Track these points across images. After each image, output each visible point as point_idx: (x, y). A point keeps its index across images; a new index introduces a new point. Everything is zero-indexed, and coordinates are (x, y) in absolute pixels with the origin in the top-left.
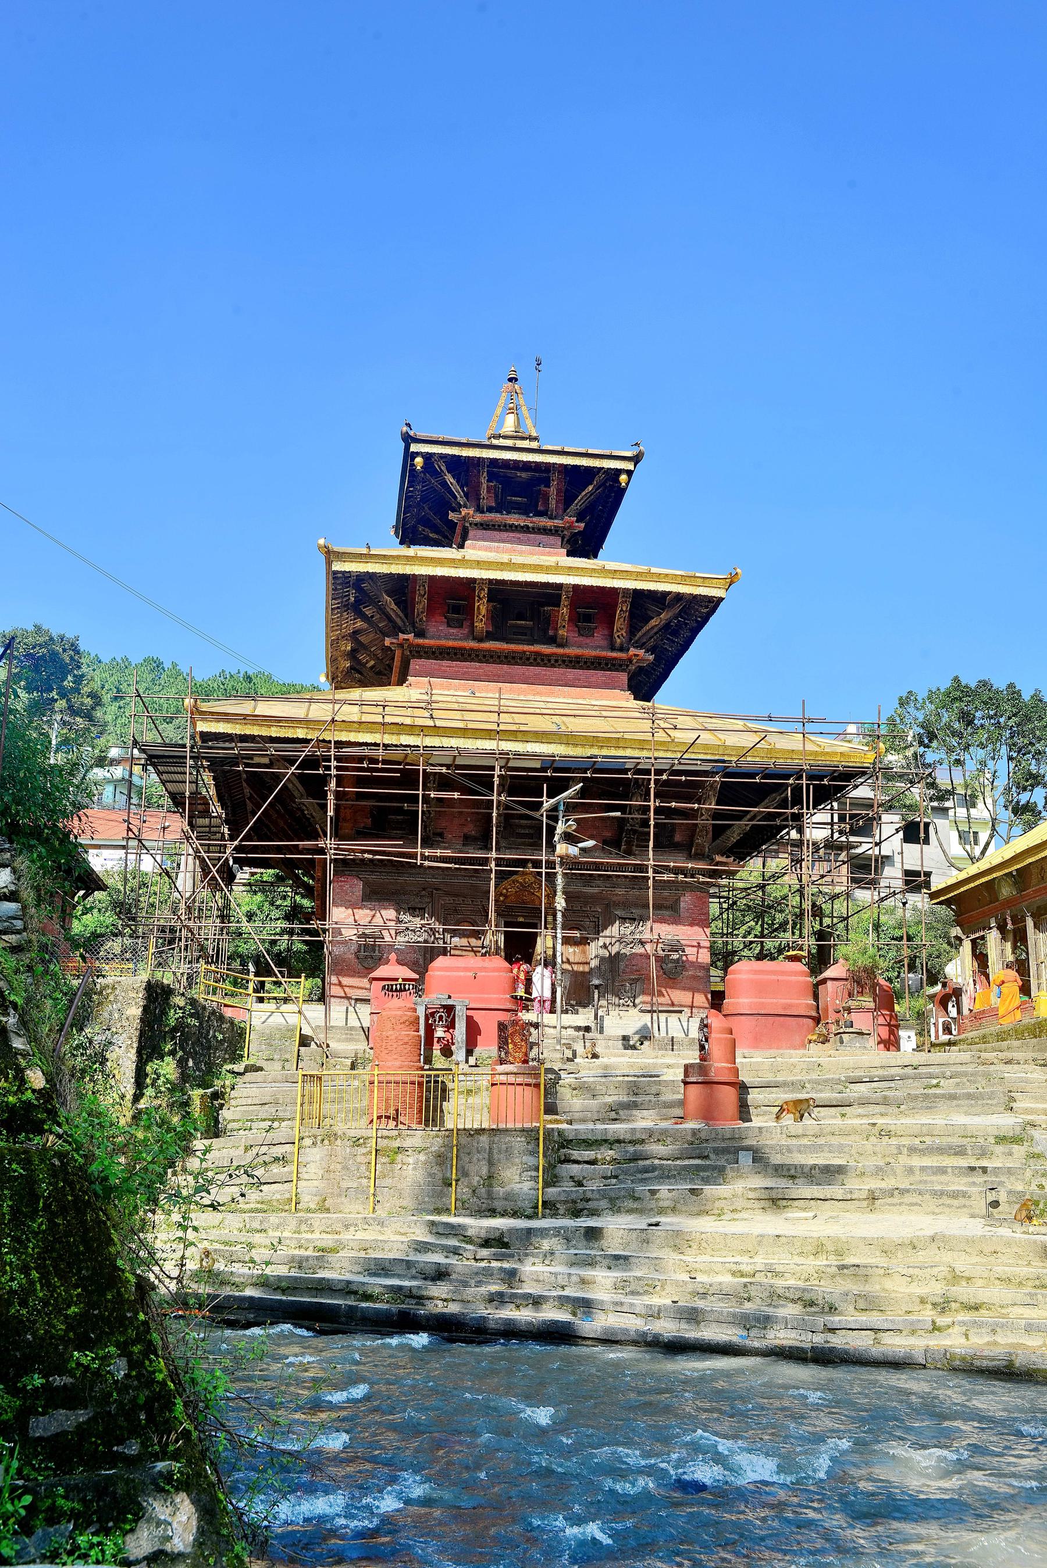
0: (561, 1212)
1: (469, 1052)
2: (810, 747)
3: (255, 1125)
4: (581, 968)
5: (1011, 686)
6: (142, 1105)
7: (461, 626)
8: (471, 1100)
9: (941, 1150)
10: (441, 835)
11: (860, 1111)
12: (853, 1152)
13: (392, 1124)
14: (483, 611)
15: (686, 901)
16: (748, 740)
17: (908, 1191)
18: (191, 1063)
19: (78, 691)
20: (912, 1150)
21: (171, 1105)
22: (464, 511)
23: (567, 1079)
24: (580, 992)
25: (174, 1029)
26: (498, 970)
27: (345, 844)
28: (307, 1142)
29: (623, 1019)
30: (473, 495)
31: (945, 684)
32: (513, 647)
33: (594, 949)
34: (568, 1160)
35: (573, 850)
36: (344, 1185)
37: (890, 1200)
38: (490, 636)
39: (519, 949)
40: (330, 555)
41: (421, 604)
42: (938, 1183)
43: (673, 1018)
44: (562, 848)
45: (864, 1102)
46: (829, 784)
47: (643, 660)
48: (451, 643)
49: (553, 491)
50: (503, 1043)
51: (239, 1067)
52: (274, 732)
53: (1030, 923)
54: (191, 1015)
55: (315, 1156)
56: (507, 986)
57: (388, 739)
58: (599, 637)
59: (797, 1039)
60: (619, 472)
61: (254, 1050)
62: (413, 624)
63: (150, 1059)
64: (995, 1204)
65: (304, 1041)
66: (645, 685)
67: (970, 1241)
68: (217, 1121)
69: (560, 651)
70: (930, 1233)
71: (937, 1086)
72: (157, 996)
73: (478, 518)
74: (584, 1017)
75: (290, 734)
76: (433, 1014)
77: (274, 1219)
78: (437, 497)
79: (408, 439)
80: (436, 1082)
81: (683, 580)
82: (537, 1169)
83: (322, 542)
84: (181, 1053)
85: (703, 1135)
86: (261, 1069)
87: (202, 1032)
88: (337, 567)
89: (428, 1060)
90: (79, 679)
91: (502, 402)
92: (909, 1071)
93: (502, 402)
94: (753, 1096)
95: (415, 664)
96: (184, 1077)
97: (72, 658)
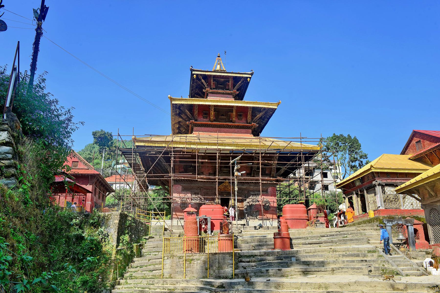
0: (240, 277)
1: (212, 232)
2: (302, 146)
3: (151, 254)
4: (242, 209)
5: (349, 135)
6: (119, 248)
7: (207, 118)
8: (213, 245)
10: (202, 173)
11: (325, 245)
12: (326, 257)
13: (190, 252)
14: (213, 114)
15: (270, 189)
16: (285, 144)
17: (344, 268)
18: (133, 236)
19: (112, 146)
20: (343, 256)
21: (127, 248)
22: (207, 89)
23: (240, 238)
24: (242, 215)
25: (128, 227)
26: (219, 208)
27: (176, 174)
28: (166, 258)
29: (254, 222)
30: (209, 85)
31: (331, 135)
32: (220, 123)
33: (245, 203)
34: (241, 261)
35: (239, 174)
36: (177, 270)
37: (338, 271)
39: (225, 203)
40: (172, 99)
41: (196, 112)
42: (352, 265)
43: (268, 221)
44: (236, 173)
45: (326, 242)
46: (309, 155)
47: (256, 126)
48: (204, 123)
49: (230, 83)
50: (221, 228)
51: (147, 237)
52: (156, 145)
53: (365, 192)
54: (133, 223)
55: (168, 262)
56: (222, 213)
57: (187, 146)
58: (244, 120)
59: (303, 226)
60: (247, 78)
61: (152, 232)
62: (194, 118)
63: (121, 235)
64: (370, 271)
65: (166, 230)
66: (256, 133)
67: (367, 283)
68: (141, 253)
70: (354, 281)
71: (346, 237)
72: (123, 217)
73: (211, 91)
74: (243, 222)
75: (161, 145)
76: (201, 221)
77: (156, 280)
78: (200, 85)
79: (192, 70)
80: (202, 240)
81: (266, 104)
82: (232, 264)
83: (169, 96)
84: (130, 233)
85: (280, 253)
86: (154, 238)
87: (137, 227)
88: (173, 102)
89: (200, 234)
90: (112, 143)
91: (216, 62)
92: (338, 233)
93: (216, 62)
94: (294, 241)
95: (195, 128)
96: (131, 240)
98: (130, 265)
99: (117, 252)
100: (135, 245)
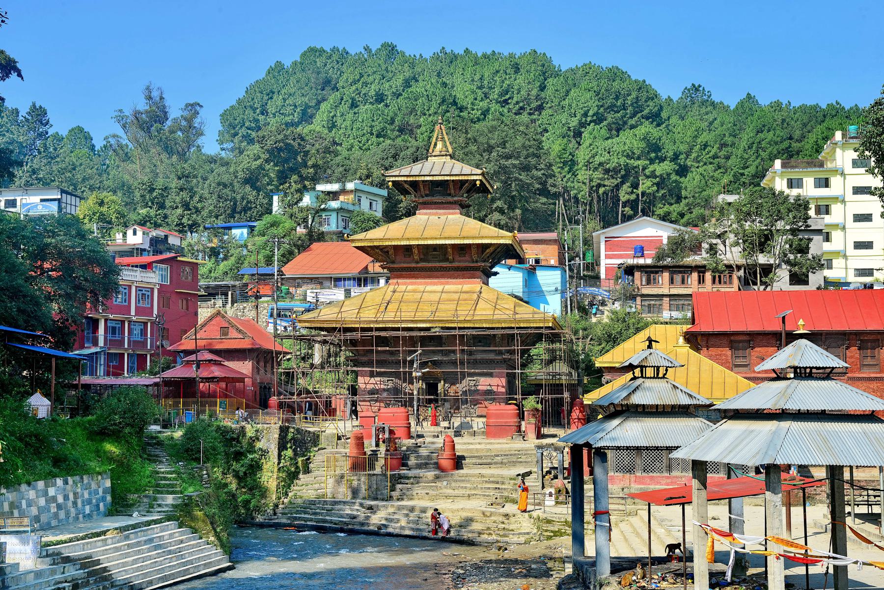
6: (281, 465)
9: (493, 482)
19: (306, 166)
21: (291, 465)
32: (430, 265)
34: (401, 483)
38: (422, 260)
41: (391, 252)
45: (496, 463)
58: (467, 258)
69: (450, 265)
90: (306, 153)
96: (296, 454)
97: (299, 144)
98: (295, 481)
99: (279, 469)
100: (300, 460)
